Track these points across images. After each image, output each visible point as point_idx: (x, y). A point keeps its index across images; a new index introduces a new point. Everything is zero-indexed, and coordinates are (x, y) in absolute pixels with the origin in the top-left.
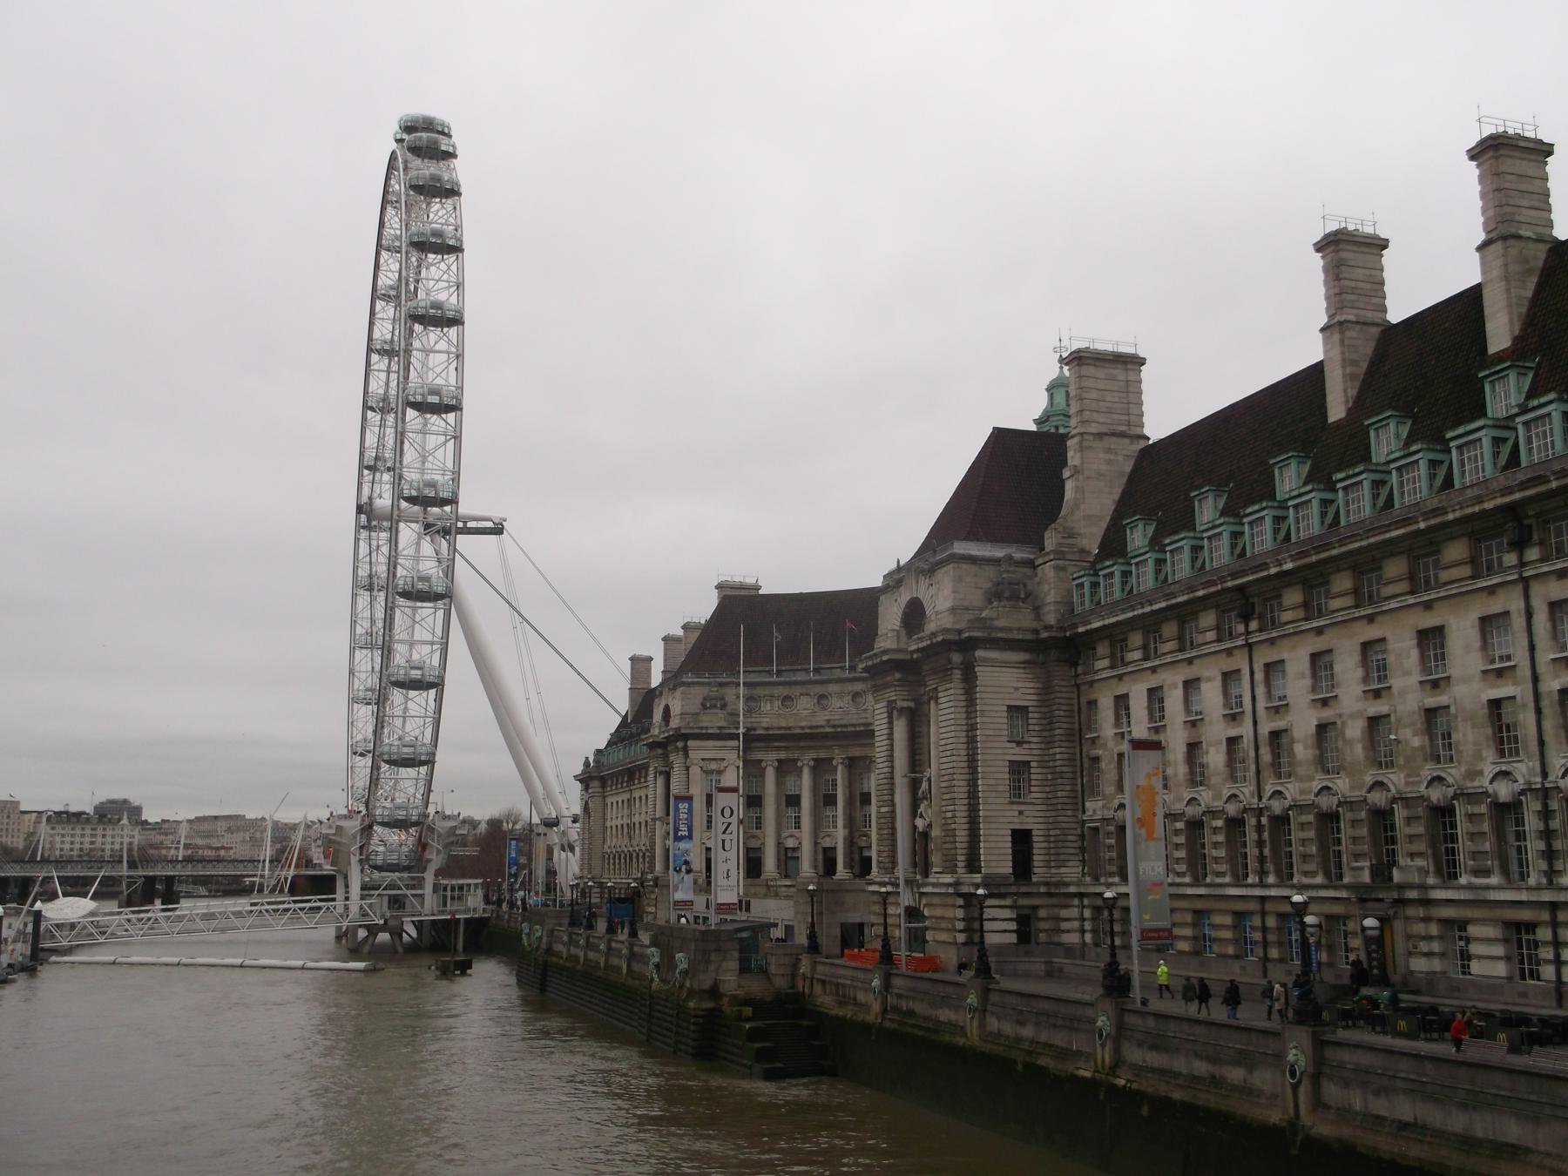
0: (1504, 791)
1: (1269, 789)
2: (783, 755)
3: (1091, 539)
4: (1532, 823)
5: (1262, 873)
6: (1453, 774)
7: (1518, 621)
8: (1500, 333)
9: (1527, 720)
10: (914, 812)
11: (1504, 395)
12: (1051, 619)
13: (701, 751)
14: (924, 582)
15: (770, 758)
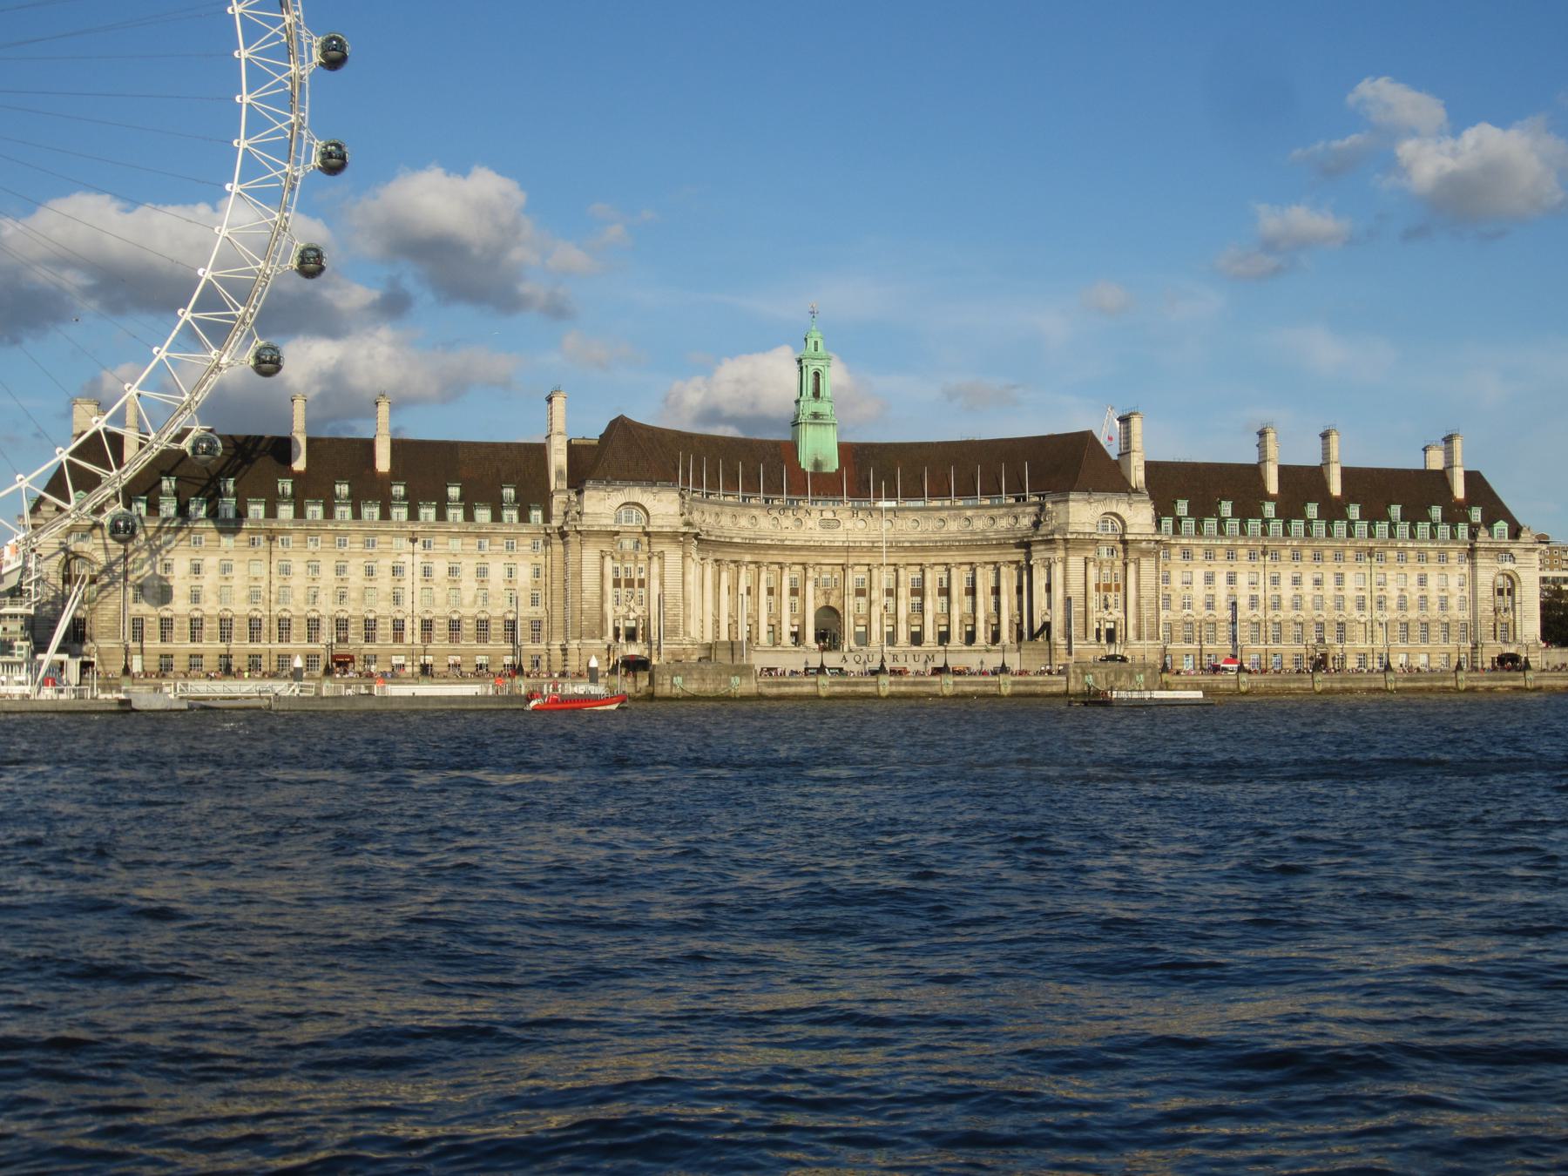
11: (1354, 511)
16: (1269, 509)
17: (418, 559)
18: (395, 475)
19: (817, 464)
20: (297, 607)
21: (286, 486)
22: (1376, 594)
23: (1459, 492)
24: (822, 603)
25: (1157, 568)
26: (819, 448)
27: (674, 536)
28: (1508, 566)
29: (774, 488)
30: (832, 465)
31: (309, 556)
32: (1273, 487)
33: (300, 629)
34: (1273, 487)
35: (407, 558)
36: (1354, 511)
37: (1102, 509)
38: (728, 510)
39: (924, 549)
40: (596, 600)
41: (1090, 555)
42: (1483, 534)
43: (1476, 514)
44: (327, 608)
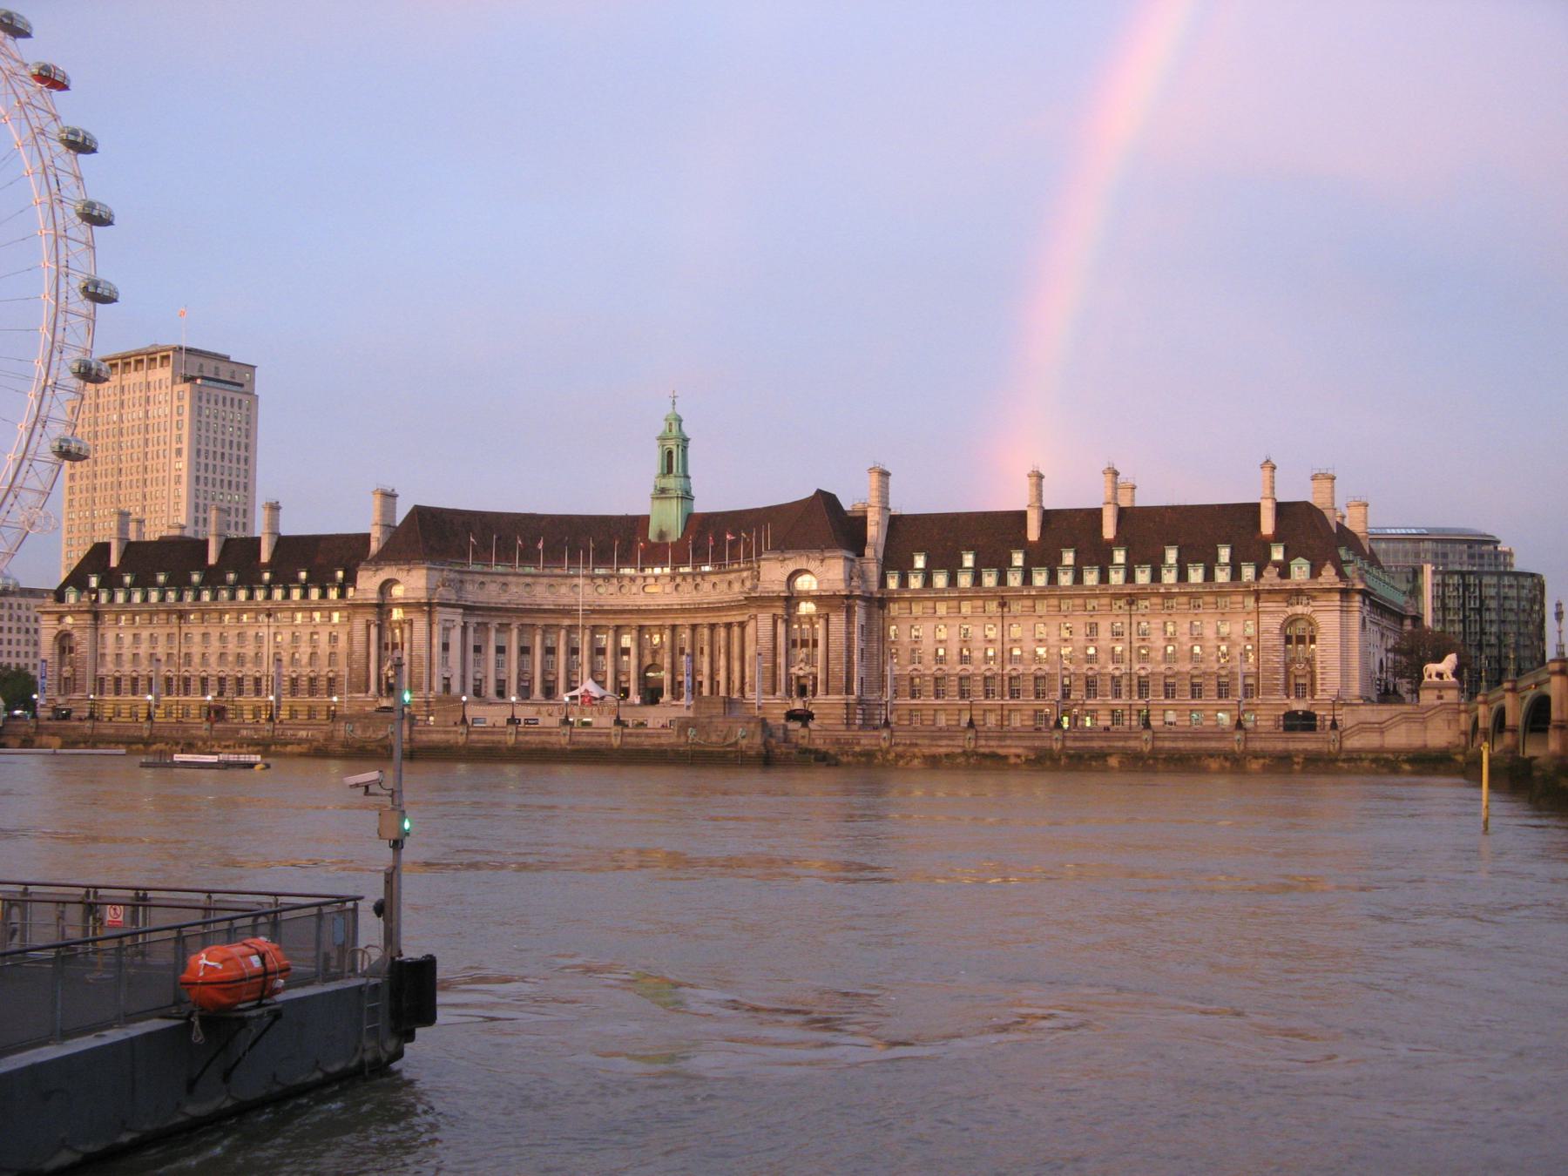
0: (1117, 673)
1: (1008, 668)
2: (480, 620)
3: (880, 555)
4: (1124, 682)
5: (1002, 697)
6: (1096, 667)
7: (1127, 626)
8: (1109, 531)
9: (1127, 654)
10: (788, 666)
11: (1119, 557)
12: (874, 587)
13: (441, 615)
14: (818, 563)
15: (473, 621)
16: (1018, 559)
17: (272, 630)
18: (268, 567)
19: (662, 535)
20: (196, 670)
21: (196, 578)
22: (1136, 645)
23: (1267, 526)
24: (648, 660)
25: (849, 621)
26: (667, 520)
27: (418, 606)
28: (1299, 609)
29: (603, 558)
30: (675, 534)
31: (203, 630)
32: (1033, 534)
33: (195, 684)
34: (1033, 534)
35: (265, 630)
36: (1119, 557)
37: (791, 567)
38: (545, 580)
39: (719, 609)
40: (363, 661)
41: (780, 612)
42: (1271, 577)
43: (1278, 554)
44: (214, 669)
